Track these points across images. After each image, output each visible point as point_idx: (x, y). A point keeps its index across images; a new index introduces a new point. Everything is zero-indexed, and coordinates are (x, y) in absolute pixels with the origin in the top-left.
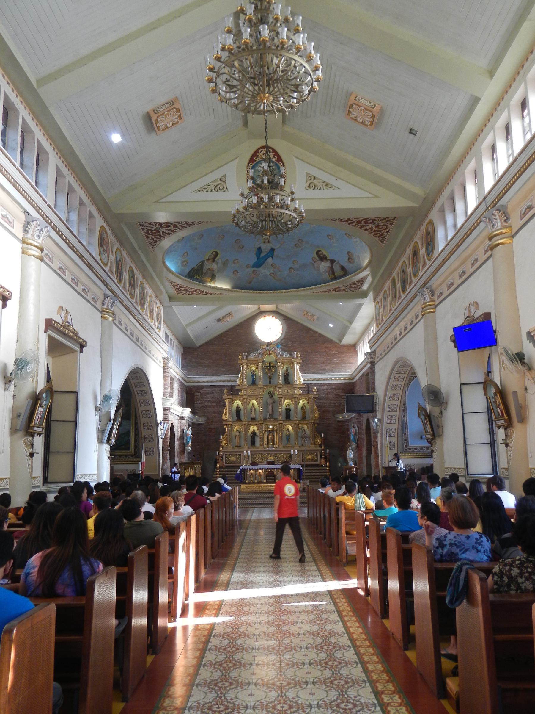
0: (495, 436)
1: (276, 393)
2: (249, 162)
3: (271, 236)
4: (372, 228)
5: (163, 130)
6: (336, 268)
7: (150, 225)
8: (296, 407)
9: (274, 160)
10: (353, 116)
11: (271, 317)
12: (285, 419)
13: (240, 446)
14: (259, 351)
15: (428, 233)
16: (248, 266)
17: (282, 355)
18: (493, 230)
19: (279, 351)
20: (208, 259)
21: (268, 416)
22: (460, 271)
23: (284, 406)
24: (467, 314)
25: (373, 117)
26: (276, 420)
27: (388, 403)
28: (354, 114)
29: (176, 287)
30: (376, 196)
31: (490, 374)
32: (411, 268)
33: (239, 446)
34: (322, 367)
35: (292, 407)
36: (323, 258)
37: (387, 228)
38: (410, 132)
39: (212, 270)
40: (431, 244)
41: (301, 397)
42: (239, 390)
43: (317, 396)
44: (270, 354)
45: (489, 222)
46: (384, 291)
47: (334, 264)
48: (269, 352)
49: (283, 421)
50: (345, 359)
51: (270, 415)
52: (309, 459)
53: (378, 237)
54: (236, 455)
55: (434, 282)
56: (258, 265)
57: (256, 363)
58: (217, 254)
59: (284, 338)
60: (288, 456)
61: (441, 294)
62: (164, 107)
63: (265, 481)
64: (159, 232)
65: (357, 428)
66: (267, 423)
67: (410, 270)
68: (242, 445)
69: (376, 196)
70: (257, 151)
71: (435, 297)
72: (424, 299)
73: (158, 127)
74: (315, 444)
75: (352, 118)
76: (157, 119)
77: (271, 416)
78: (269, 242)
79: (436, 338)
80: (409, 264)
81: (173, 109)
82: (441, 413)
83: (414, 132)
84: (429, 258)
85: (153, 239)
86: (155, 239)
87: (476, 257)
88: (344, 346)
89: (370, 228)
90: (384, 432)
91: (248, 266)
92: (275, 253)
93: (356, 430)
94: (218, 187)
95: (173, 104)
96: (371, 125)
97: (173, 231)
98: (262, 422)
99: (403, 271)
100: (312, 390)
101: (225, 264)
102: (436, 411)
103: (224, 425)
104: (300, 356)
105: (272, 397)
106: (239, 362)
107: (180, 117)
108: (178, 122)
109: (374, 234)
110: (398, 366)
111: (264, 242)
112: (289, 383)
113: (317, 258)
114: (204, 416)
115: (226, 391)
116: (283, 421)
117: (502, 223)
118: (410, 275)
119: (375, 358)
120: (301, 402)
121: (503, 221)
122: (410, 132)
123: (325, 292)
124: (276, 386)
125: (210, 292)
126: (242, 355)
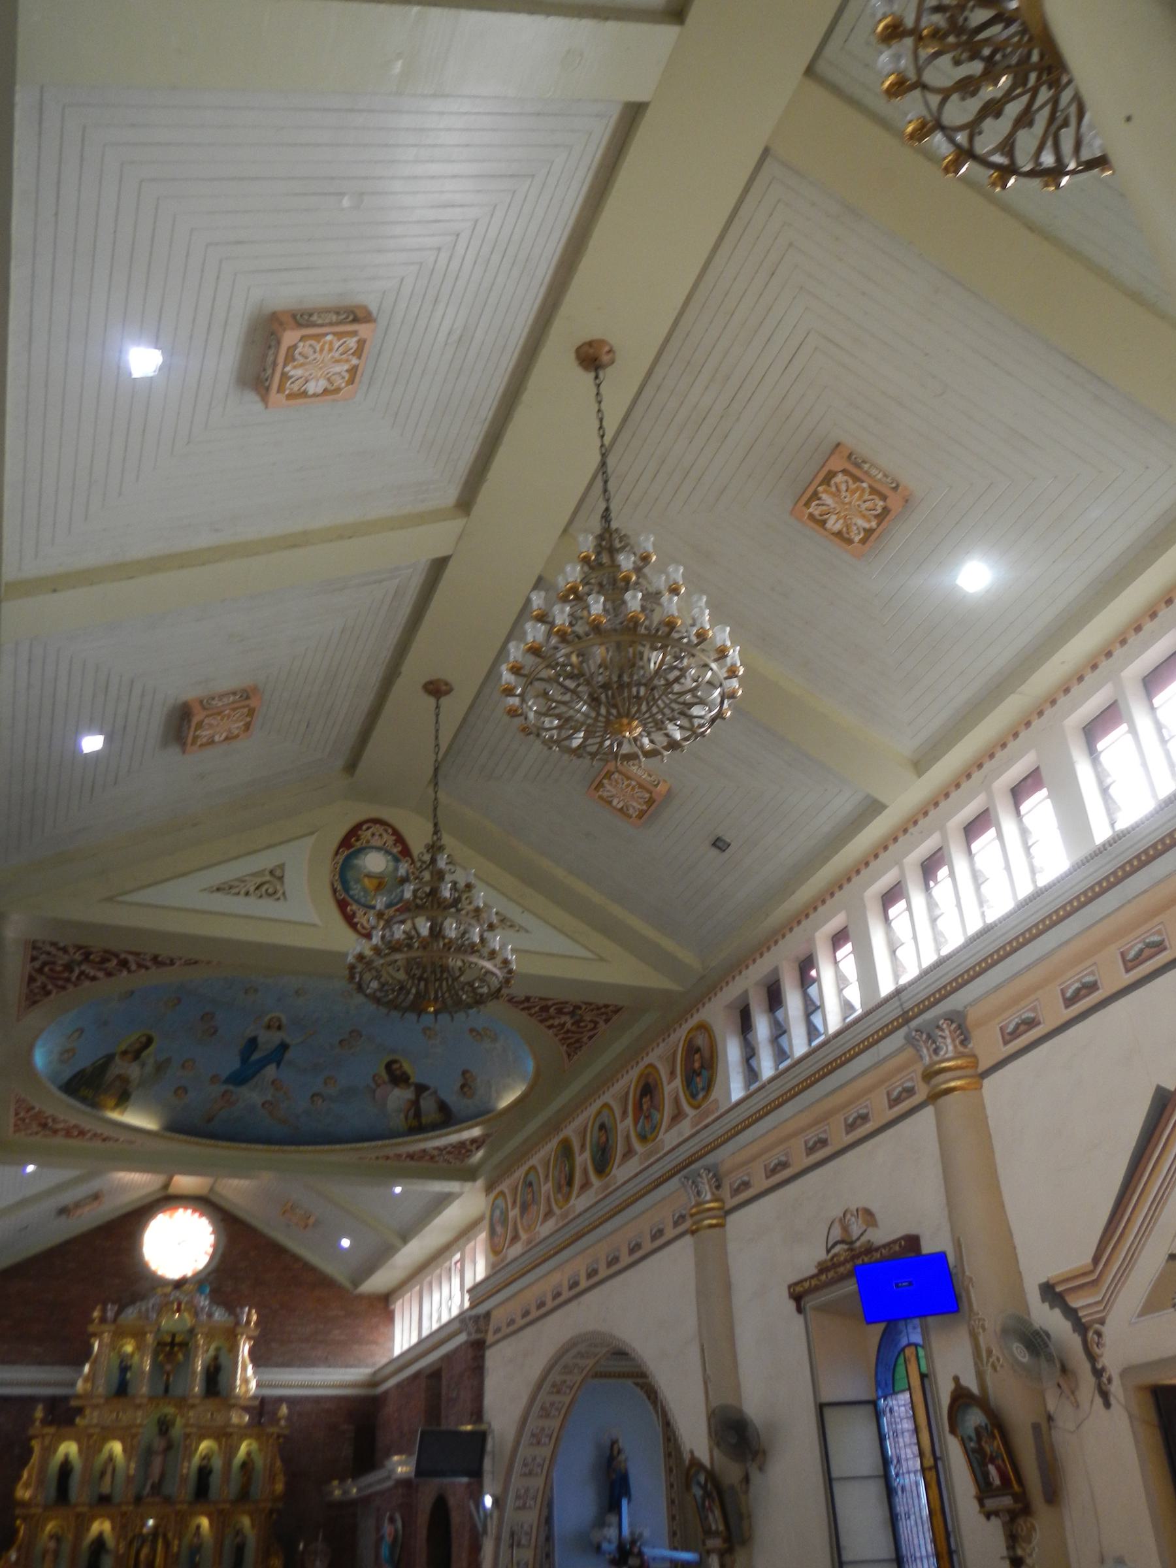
0: (952, 1540)
1: (179, 1422)
2: (339, 848)
3: (440, 1017)
4: (565, 1024)
6: (428, 1104)
7: (60, 953)
8: (228, 1462)
9: (395, 850)
10: (605, 794)
11: (189, 1211)
14: (152, 1302)
15: (692, 1050)
16: (214, 1079)
17: (210, 1315)
18: (936, 1058)
19: (203, 1302)
20: (124, 1053)
21: (148, 1488)
22: (812, 1136)
23: (196, 1460)
24: (837, 1233)
25: (650, 802)
26: (168, 1500)
27: (523, 1452)
28: (609, 789)
29: (22, 1115)
30: (602, 959)
31: (926, 1381)
32: (629, 1121)
35: (217, 1463)
36: (398, 1078)
37: (595, 1028)
38: (714, 844)
39: (124, 1080)
40: (705, 1073)
41: (244, 1432)
42: (80, 1411)
43: (286, 1432)
44: (178, 1310)
45: (926, 1042)
46: (525, 1168)
47: (425, 1094)
48: (179, 1305)
53: (567, 1046)
55: (724, 1156)
56: (239, 1079)
58: (149, 1041)
61: (746, 1185)
62: (226, 700)
64: (72, 971)
65: (399, 1524)
67: (625, 1126)
69: (602, 959)
70: (358, 826)
71: (726, 1192)
72: (699, 1193)
73: (195, 738)
75: (601, 797)
76: (202, 721)
77: (157, 1488)
78: (279, 1028)
79: (728, 1287)
80: (625, 1113)
81: (244, 707)
82: (747, 1479)
83: (720, 844)
84: (695, 1103)
85: (44, 987)
86: (50, 987)
87: (864, 1111)
88: (361, 1297)
89: (559, 1025)
90: (505, 1535)
91: (214, 1079)
92: (289, 1055)
93: (396, 1531)
94: (264, 889)
95: (248, 698)
96: (640, 817)
97: (109, 974)
99: (602, 1127)
100: (275, 1413)
101: (160, 1068)
102: (731, 1473)
104: (254, 1318)
106: (91, 1328)
107: (247, 727)
108: (237, 736)
109: (563, 1039)
110: (574, 1352)
111: (269, 1027)
113: (386, 1077)
115: (39, 1413)
117: (955, 1047)
118: (628, 1137)
119: (486, 1331)
120: (244, 1448)
121: (957, 1042)
122: (714, 844)
123: (387, 1158)
124: (182, 1403)
125: (106, 1134)
126: (104, 1311)
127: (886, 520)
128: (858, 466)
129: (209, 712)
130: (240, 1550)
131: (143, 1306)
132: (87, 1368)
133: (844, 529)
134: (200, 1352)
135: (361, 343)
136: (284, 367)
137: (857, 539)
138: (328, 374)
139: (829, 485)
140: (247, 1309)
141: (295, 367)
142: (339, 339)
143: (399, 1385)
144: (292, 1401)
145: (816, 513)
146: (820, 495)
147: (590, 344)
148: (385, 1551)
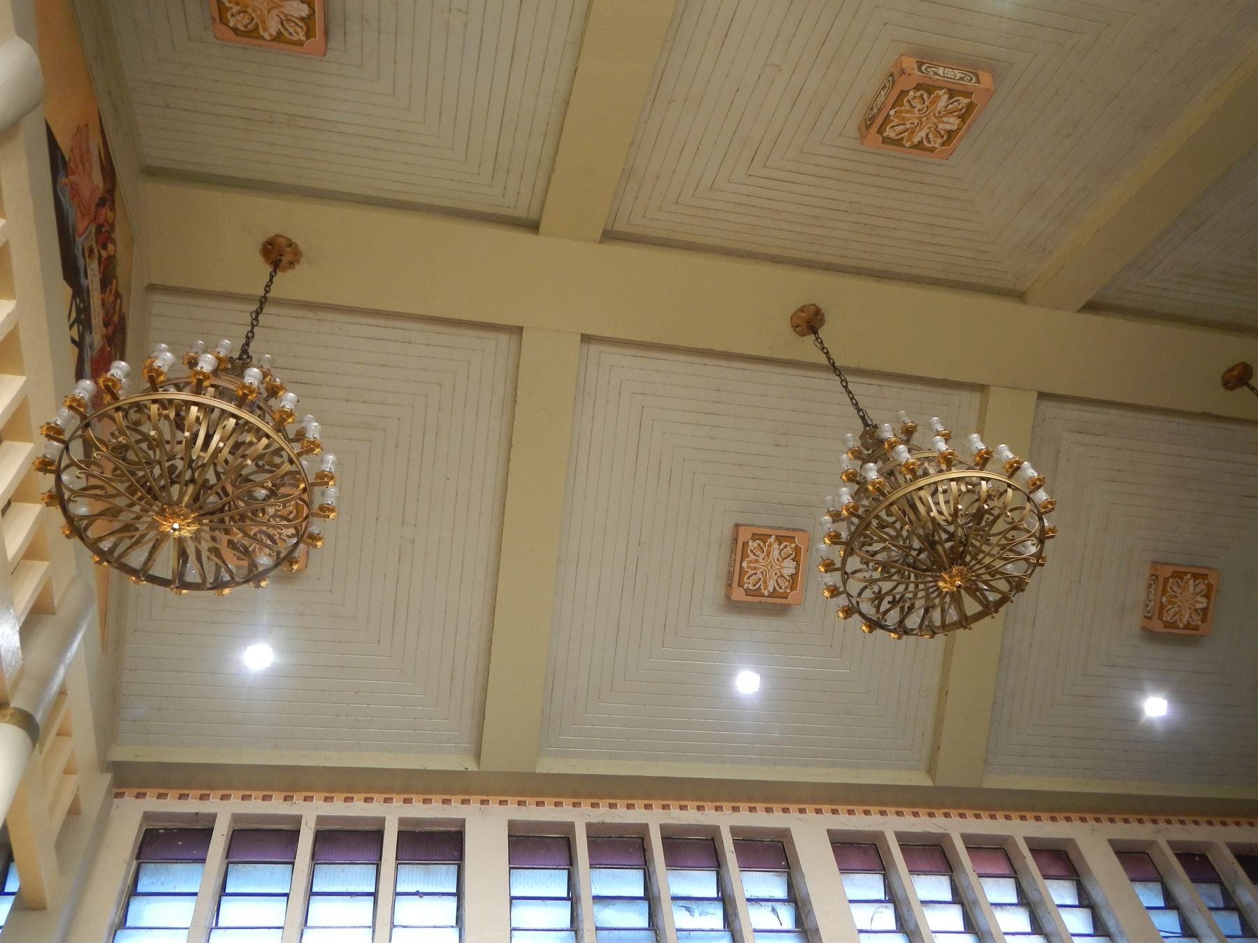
5: (1204, 620)
62: (1152, 597)
95: (1157, 577)
108: (1209, 586)
127: (934, 84)
128: (873, 119)
129: (1156, 615)
133: (956, 113)
135: (755, 537)
136: (765, 596)
137: (964, 101)
138: (778, 560)
139: (902, 139)
141: (766, 588)
142: (748, 556)
145: (939, 141)
146: (916, 143)
147: (795, 327)
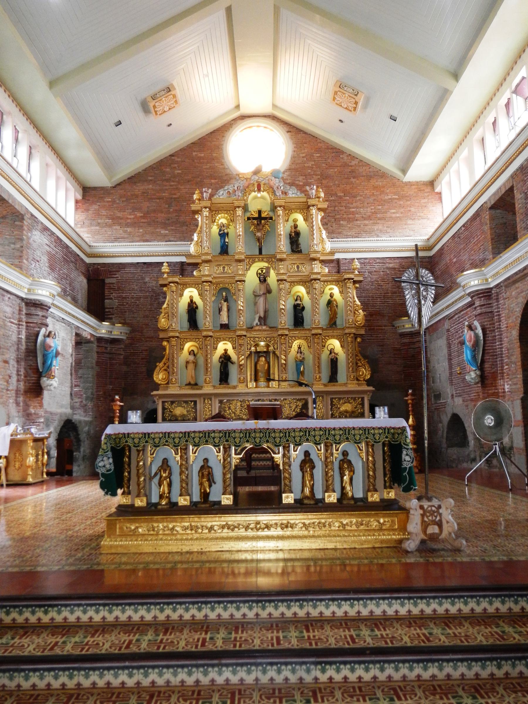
8: (315, 301)
12: (291, 327)
13: (196, 384)
17: (285, 193)
21: (257, 321)
26: (274, 328)
33: (195, 385)
34: (366, 225)
35: (306, 301)
44: (259, 190)
49: (289, 330)
50: (413, 209)
51: (260, 318)
52: (346, 411)
54: (186, 402)
57: (231, 209)
59: (289, 169)
60: (300, 404)
63: (227, 500)
65: (479, 331)
66: (254, 334)
68: (201, 382)
74: (358, 380)
77: (263, 320)
88: (410, 184)
93: (477, 336)
98: (244, 333)
103: (163, 339)
104: (322, 195)
105: (265, 280)
112: (300, 252)
114: (124, 324)
116: (289, 330)
130: (334, 363)
131: (230, 188)
132: (195, 237)
134: (281, 221)
140: (315, 187)
143: (453, 236)
144: (363, 262)
148: (467, 354)
